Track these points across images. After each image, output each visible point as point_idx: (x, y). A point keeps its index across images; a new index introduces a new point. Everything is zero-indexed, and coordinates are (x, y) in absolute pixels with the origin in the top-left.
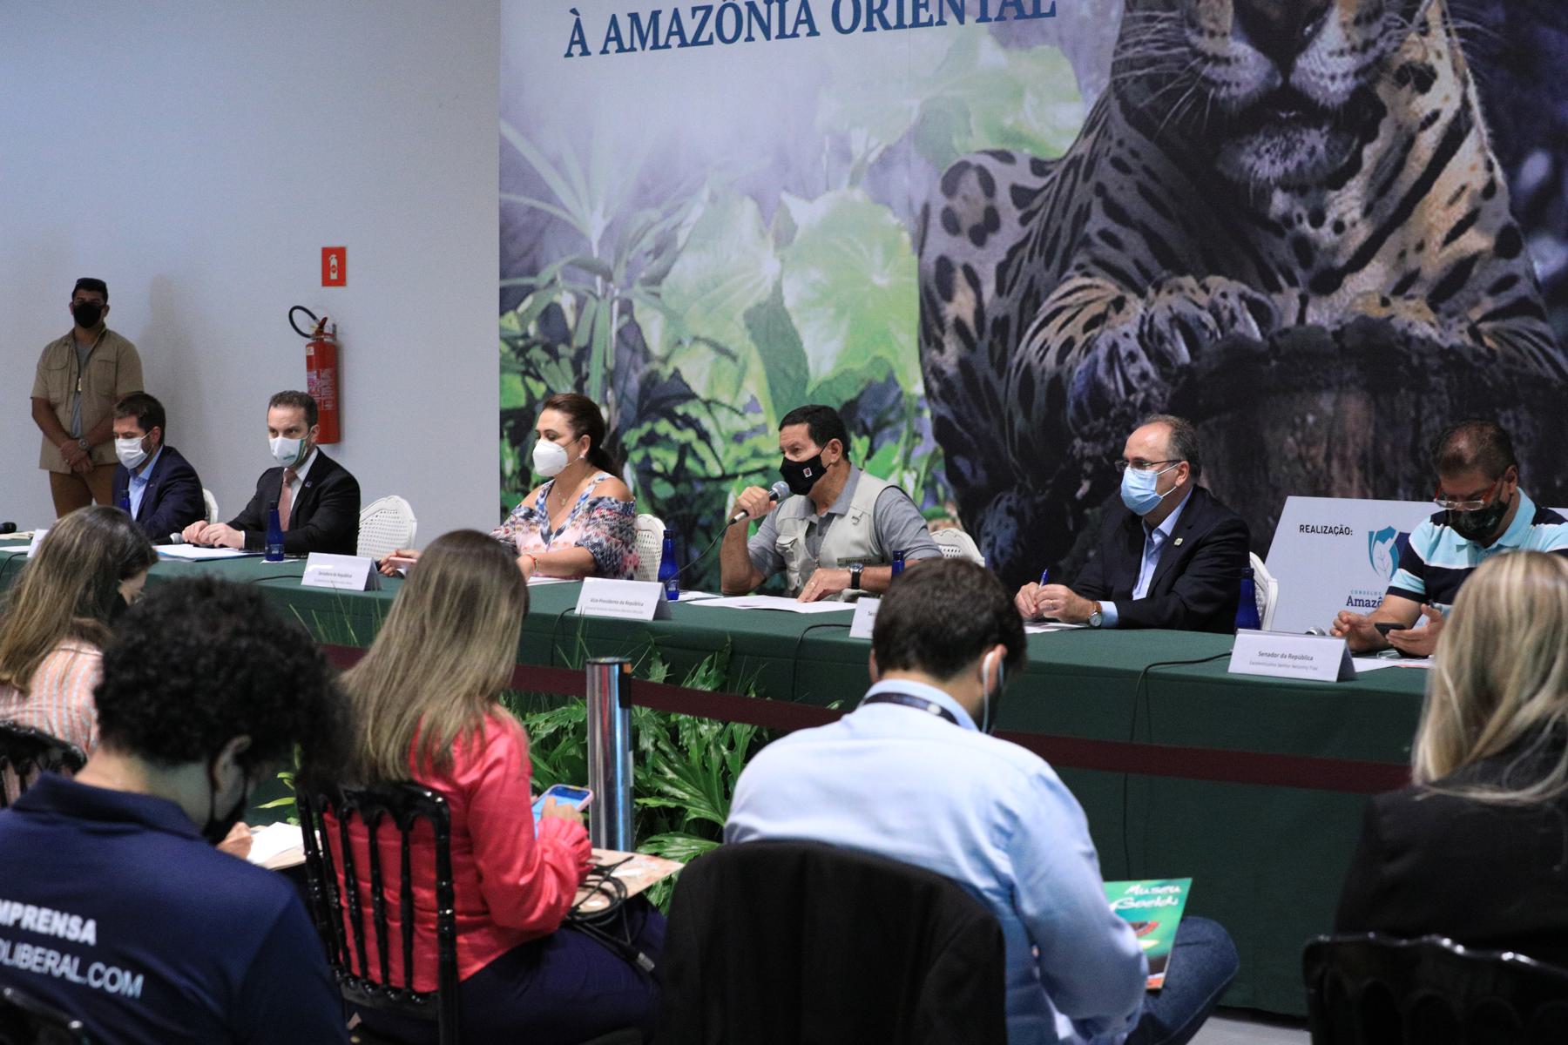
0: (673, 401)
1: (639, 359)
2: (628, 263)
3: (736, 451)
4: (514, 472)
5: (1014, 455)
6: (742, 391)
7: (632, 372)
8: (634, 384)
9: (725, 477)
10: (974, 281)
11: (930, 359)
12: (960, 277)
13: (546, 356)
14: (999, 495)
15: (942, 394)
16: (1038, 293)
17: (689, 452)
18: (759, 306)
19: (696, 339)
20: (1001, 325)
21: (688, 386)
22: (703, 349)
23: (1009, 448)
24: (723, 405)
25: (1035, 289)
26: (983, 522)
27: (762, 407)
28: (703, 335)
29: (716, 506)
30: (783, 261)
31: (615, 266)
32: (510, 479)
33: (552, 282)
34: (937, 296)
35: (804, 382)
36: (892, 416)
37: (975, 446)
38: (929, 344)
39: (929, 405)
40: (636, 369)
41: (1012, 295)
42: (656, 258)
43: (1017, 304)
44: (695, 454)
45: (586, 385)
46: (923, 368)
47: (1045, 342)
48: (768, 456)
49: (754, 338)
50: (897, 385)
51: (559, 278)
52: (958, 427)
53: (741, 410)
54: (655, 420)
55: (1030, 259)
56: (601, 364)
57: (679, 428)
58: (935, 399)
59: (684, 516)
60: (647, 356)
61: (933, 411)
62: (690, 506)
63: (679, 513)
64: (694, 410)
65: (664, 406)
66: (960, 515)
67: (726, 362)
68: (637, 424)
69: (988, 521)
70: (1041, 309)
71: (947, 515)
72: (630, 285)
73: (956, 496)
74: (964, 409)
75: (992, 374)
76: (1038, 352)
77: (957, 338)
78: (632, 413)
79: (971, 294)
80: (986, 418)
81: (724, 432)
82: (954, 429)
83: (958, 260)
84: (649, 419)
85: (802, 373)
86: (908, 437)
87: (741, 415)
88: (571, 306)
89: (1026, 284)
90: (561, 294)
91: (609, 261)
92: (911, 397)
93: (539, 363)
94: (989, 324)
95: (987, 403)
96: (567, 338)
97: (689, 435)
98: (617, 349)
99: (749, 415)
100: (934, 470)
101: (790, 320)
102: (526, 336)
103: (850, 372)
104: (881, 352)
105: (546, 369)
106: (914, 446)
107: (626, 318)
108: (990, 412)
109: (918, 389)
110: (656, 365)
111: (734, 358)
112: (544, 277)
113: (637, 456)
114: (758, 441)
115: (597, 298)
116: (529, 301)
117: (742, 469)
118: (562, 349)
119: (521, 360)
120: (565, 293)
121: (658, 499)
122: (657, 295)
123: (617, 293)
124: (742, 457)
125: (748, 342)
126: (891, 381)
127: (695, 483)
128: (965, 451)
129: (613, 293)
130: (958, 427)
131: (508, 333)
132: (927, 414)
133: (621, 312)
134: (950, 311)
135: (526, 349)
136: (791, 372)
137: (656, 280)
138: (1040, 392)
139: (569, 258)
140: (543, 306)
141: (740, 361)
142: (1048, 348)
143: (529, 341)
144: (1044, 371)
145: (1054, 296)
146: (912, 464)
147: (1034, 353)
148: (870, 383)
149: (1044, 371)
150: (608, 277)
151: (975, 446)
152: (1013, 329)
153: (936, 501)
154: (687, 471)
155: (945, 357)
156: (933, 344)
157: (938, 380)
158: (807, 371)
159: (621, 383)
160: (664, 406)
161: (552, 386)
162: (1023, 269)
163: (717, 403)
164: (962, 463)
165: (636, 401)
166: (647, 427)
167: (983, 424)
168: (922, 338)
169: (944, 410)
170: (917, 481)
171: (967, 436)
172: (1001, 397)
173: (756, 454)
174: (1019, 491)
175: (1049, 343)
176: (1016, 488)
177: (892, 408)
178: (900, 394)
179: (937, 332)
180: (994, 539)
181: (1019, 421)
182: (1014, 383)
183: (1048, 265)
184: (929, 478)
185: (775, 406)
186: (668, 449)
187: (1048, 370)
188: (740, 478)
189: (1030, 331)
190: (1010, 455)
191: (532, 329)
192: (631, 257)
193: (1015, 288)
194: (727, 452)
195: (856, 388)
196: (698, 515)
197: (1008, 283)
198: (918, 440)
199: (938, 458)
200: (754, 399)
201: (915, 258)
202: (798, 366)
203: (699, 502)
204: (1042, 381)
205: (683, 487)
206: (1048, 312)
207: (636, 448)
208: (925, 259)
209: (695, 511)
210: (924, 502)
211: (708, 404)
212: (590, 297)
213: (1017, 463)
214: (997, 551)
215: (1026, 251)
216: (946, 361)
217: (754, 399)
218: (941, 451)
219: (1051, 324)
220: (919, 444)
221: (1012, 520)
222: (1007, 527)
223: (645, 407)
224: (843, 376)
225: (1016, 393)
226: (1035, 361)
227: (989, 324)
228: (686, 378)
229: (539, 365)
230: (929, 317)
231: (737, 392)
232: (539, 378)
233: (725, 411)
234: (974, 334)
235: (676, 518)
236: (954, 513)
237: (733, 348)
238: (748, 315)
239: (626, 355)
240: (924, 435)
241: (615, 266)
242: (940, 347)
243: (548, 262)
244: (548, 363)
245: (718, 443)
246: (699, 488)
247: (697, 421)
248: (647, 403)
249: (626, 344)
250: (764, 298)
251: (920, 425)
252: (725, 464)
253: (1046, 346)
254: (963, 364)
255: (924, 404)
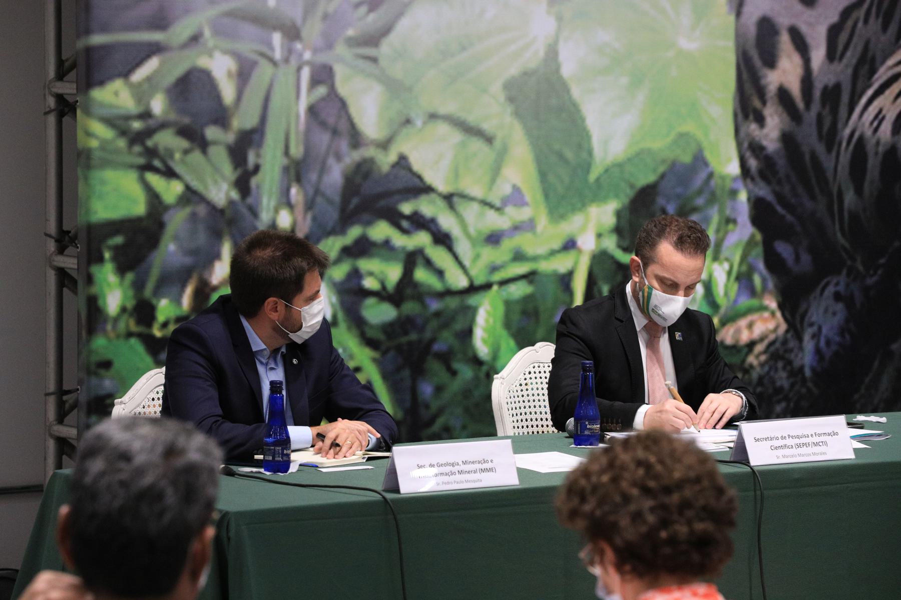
0: (396, 197)
1: (344, 145)
2: (326, 17)
3: (489, 255)
4: (124, 310)
5: (843, 234)
6: (499, 181)
7: (331, 161)
8: (335, 176)
9: (473, 289)
10: (801, 45)
11: (748, 135)
12: (785, 40)
13: (184, 144)
14: (825, 281)
15: (763, 175)
16: (873, 59)
17: (420, 261)
18: (526, 74)
19: (433, 116)
20: (832, 94)
21: (419, 177)
22: (443, 128)
23: (837, 226)
24: (472, 199)
25: (870, 54)
26: (806, 312)
27: (528, 198)
28: (443, 110)
29: (458, 326)
30: (560, 19)
31: (305, 19)
32: (116, 320)
33: (195, 39)
34: (757, 62)
35: (587, 167)
36: (700, 201)
37: (798, 229)
38: (746, 117)
39: (746, 186)
40: (339, 157)
41: (845, 61)
42: (371, 10)
43: (850, 71)
44: (429, 263)
45: (254, 182)
46: (739, 144)
47: (880, 111)
48: (535, 259)
49: (517, 114)
50: (706, 164)
51: (207, 33)
52: (779, 209)
53: (498, 203)
54: (369, 223)
55: (866, 21)
56: (279, 152)
57: (405, 231)
58: (753, 179)
59: (410, 343)
60: (356, 139)
61: (749, 193)
62: (422, 329)
63: (404, 340)
64: (427, 207)
65: (382, 203)
66: (781, 306)
67: (477, 144)
68: (341, 228)
69: (813, 309)
70: (876, 76)
71: (764, 308)
72: (330, 46)
73: (776, 286)
74: (786, 190)
75: (820, 149)
76: (872, 123)
77: (780, 109)
78: (332, 215)
79: (797, 59)
80: (813, 197)
81: (472, 231)
82: (774, 211)
83: (783, 21)
84: (358, 222)
85: (584, 155)
86: (719, 224)
87: (498, 209)
88: (230, 74)
89: (860, 49)
90: (211, 56)
91: (295, 13)
92: (723, 178)
93: (170, 153)
94: (817, 94)
95: (814, 181)
96: (221, 118)
97: (422, 239)
98: (308, 131)
99: (510, 210)
100: (750, 259)
101: (568, 91)
102: (146, 115)
103: (649, 151)
104: (688, 127)
105: (183, 161)
106: (726, 233)
107: (322, 91)
108: (817, 190)
109: (733, 168)
110: (370, 152)
111: (489, 140)
112: (181, 31)
113: (339, 272)
114: (526, 243)
115: (274, 63)
116: (152, 65)
117: (497, 277)
118: (212, 132)
119: (137, 149)
120: (218, 55)
121: (372, 327)
122: (374, 60)
123: (307, 56)
124: (498, 262)
125: (508, 119)
126: (700, 160)
127: (428, 300)
128: (787, 234)
129: (301, 55)
130: (779, 209)
131: (115, 112)
132: (743, 196)
133: (315, 82)
134: (773, 79)
135: (149, 133)
136: (569, 154)
137: (373, 39)
138: (873, 164)
139: (225, 7)
140: (179, 71)
141: (498, 143)
142: (883, 118)
143: (151, 122)
144: (878, 143)
145: (890, 62)
146: (725, 253)
147: (867, 124)
148: (674, 165)
149: (878, 143)
150: (292, 33)
151: (798, 229)
152: (845, 98)
153: (753, 293)
154: (416, 285)
155: (765, 131)
156: (751, 117)
157: (757, 157)
158: (590, 153)
159: (313, 177)
160: (382, 203)
161: (195, 184)
162: (857, 32)
163: (464, 197)
164: (784, 249)
165: (337, 199)
166: (355, 232)
167: (809, 205)
168: (739, 111)
169: (764, 191)
170: (729, 273)
171: (789, 218)
172: (830, 174)
173: (519, 256)
174: (848, 275)
175: (884, 112)
176: (844, 272)
177: (700, 192)
178: (711, 175)
179: (757, 103)
180: (820, 328)
181: (849, 197)
182: (845, 158)
183: (885, 27)
184: (744, 268)
185: (546, 196)
186: (387, 259)
187: (883, 141)
188: (495, 288)
189: (864, 100)
190: (839, 235)
191: (158, 105)
192: (331, 9)
193: (849, 54)
194: (477, 257)
195: (654, 170)
196: (433, 340)
197: (840, 47)
198: (731, 226)
199: (756, 244)
200: (516, 189)
201: (732, 18)
202: (580, 146)
203: (434, 324)
204: (876, 153)
205: (410, 307)
206: (884, 78)
207: (338, 261)
208: (744, 18)
209: (428, 335)
210: (738, 294)
211: (449, 199)
212: (263, 62)
213: (847, 245)
214: (822, 343)
215: (861, 13)
216: (767, 136)
217: (516, 189)
218: (759, 237)
219: (887, 92)
220: (733, 231)
221: (840, 307)
222: (834, 314)
223: (352, 206)
224: (638, 158)
225: (847, 170)
226: (869, 133)
227: (817, 94)
228: (417, 166)
229: (171, 156)
230: (748, 87)
231: (493, 181)
232: (170, 174)
233: (475, 206)
234: (800, 105)
235: (399, 349)
236: (773, 305)
237: (486, 126)
238: (509, 86)
239: (323, 139)
240: (739, 220)
241: (305, 19)
242: (760, 120)
243: (187, 11)
244: (186, 152)
245: (463, 247)
246: (435, 305)
247: (433, 221)
248: (355, 201)
249: (323, 124)
250: (533, 65)
251: (734, 209)
252: (473, 272)
253: (880, 116)
254: (787, 139)
255: (740, 185)
